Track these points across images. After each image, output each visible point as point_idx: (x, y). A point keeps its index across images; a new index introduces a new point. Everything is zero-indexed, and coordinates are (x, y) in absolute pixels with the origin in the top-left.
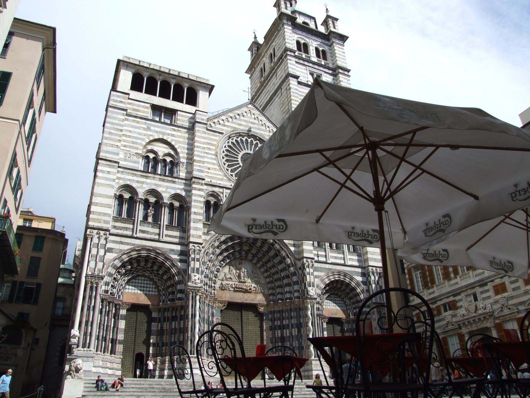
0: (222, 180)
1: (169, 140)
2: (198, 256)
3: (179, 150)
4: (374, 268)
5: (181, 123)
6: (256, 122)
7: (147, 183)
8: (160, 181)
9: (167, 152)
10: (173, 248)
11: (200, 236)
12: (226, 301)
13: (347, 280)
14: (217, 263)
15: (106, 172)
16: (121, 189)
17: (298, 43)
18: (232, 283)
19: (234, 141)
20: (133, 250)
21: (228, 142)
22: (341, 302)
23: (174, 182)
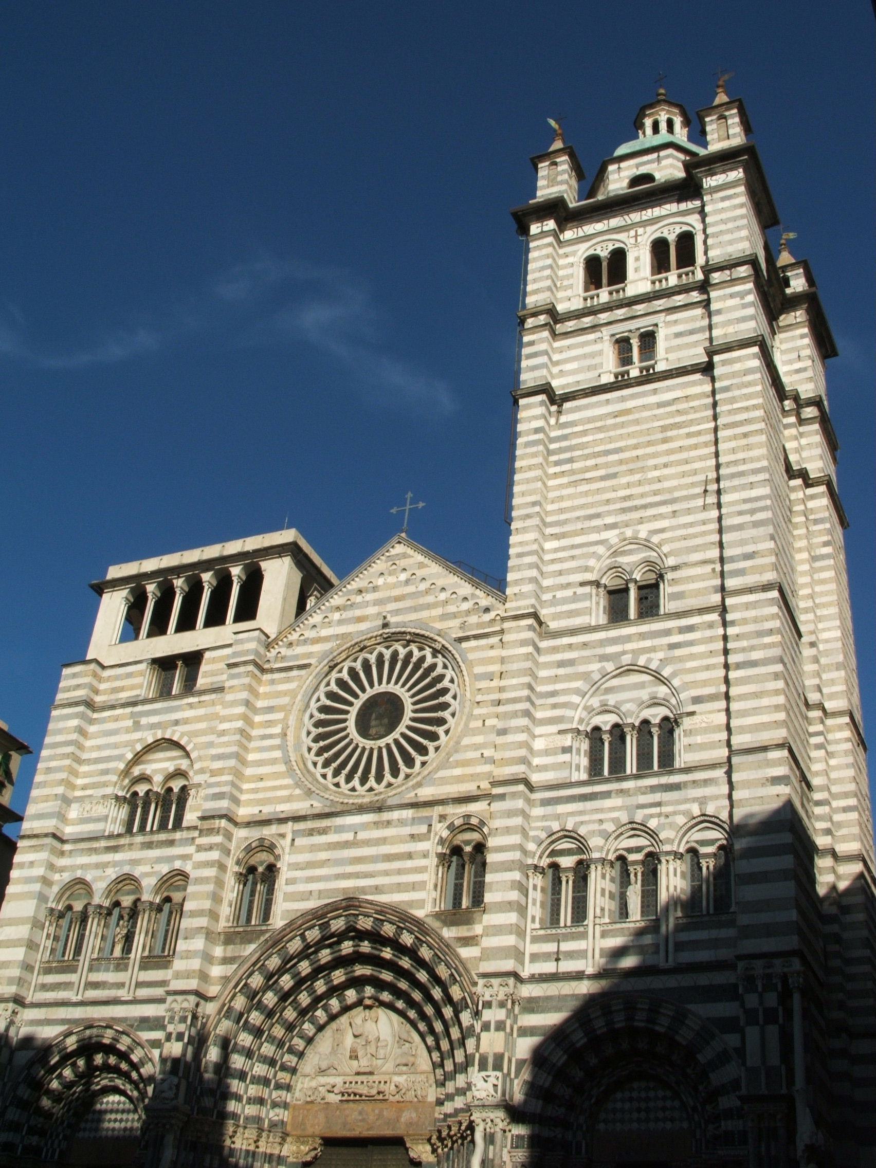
0: (289, 799)
1: (175, 738)
2: (182, 1027)
3: (193, 756)
4: (759, 963)
5: (209, 680)
6: (411, 589)
7: (115, 864)
9: (171, 769)
10: (146, 1014)
11: (194, 971)
12: (313, 1136)
13: (662, 1025)
14: (278, 1031)
15: (27, 865)
16: (68, 893)
17: (592, 264)
18: (339, 1080)
19: (345, 675)
20: (68, 1034)
21: (328, 684)
22: (669, 1103)
23: (171, 843)
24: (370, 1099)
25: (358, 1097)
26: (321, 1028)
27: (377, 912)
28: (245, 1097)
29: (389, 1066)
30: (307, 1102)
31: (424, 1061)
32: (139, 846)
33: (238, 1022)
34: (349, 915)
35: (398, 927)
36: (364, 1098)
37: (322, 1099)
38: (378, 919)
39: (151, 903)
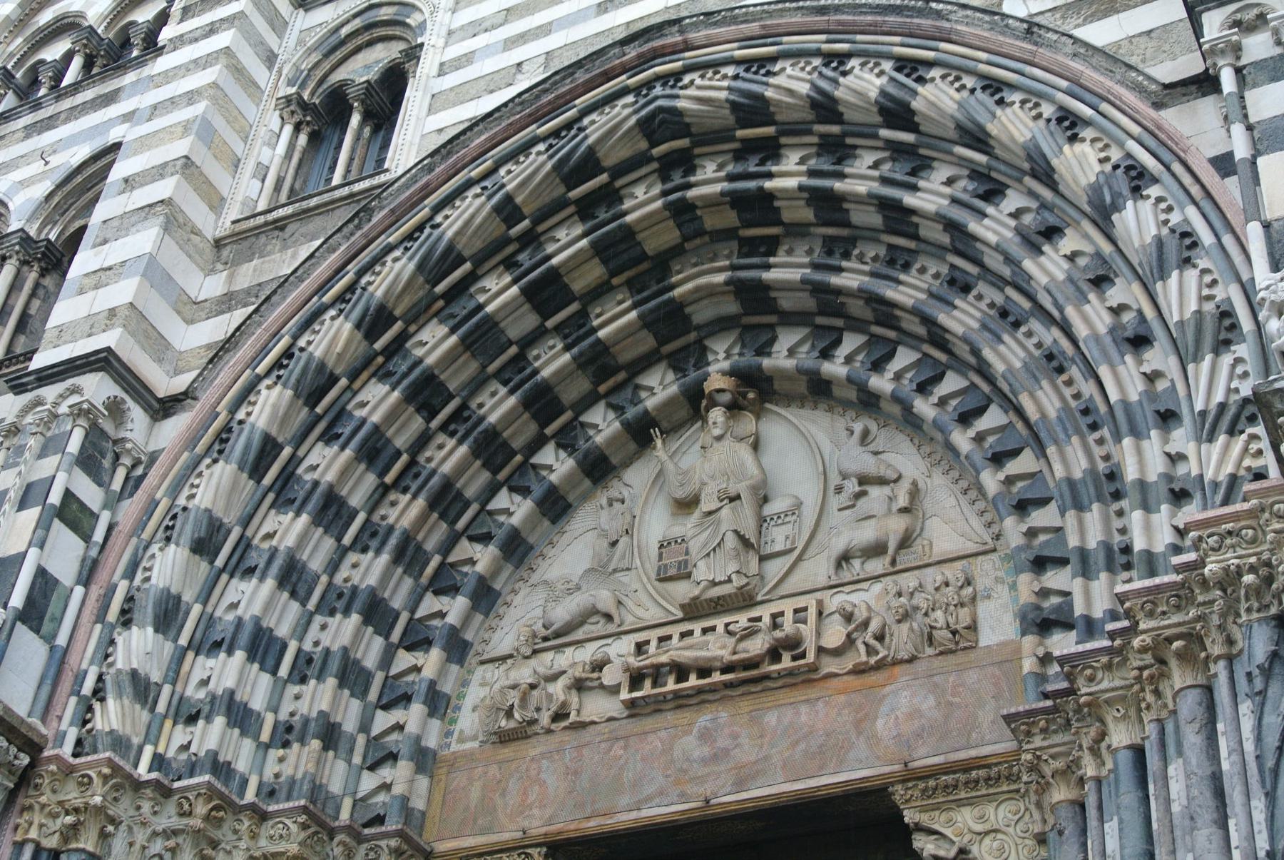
8: (27, 137)
11: (112, 312)
24: (747, 678)
25: (693, 681)
26: (555, 506)
27: (747, 41)
28: (269, 719)
29: (818, 569)
30: (505, 738)
31: (950, 526)
32: (21, 134)
33: (257, 471)
34: (649, 84)
35: (829, 58)
36: (717, 677)
37: (559, 716)
38: (747, 63)
39: (26, 240)
